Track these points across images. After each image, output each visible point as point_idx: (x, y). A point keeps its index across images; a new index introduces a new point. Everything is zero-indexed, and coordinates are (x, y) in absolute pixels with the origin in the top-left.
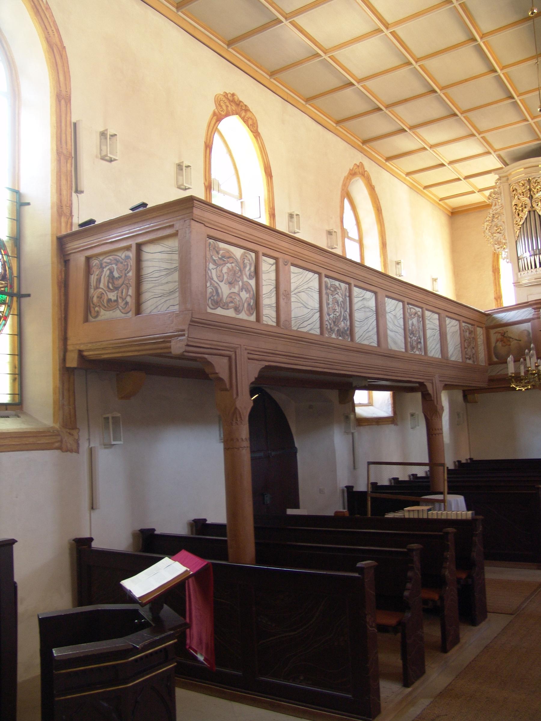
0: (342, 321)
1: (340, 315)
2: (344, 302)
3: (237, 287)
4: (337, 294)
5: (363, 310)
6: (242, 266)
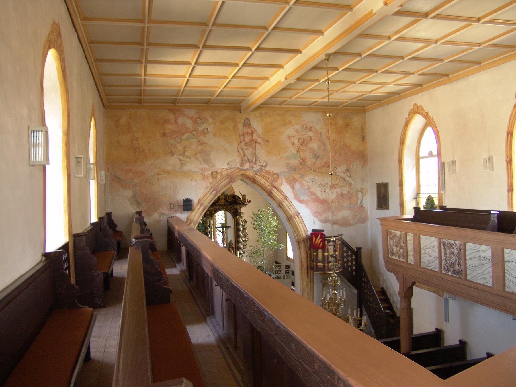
0: (457, 265)
1: (455, 262)
2: (459, 253)
3: (399, 247)
5: (478, 259)
6: (400, 239)
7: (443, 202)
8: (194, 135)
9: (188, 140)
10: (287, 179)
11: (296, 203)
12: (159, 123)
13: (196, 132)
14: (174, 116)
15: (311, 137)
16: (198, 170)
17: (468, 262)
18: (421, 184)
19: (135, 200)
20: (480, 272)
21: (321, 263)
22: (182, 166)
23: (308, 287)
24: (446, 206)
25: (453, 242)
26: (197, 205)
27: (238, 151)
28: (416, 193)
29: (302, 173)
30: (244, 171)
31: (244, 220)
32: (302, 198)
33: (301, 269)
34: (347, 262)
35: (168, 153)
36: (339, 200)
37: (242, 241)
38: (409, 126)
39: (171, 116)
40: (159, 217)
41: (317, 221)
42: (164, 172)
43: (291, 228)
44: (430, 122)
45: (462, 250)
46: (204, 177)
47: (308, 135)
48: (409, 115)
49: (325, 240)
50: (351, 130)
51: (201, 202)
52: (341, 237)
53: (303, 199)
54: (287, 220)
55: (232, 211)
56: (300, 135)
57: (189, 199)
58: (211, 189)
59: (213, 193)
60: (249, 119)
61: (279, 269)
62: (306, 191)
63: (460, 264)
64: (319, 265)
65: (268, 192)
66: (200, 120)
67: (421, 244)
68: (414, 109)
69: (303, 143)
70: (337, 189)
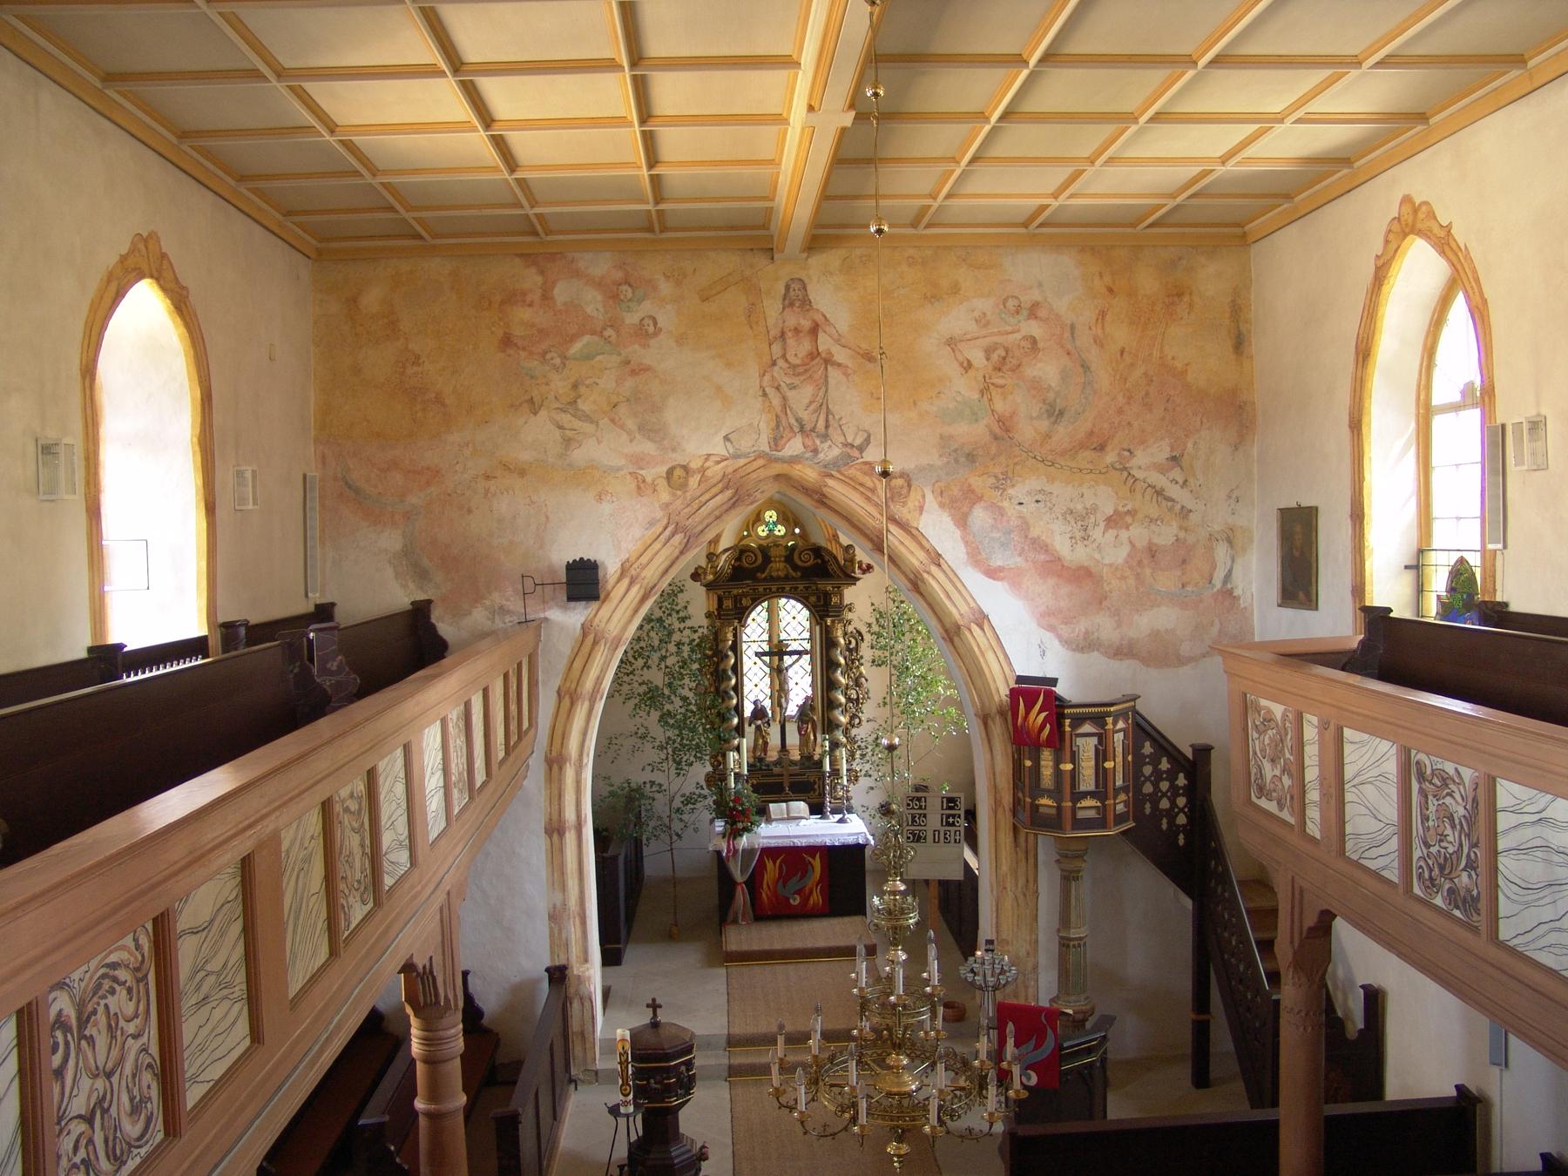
0: (1464, 870)
2: (1471, 819)
4: (1448, 794)
5: (1539, 854)
7: (1498, 587)
8: (607, 340)
9: (589, 357)
10: (942, 493)
11: (973, 580)
12: (490, 305)
13: (618, 332)
14: (539, 279)
15: (1034, 341)
16: (623, 462)
17: (1504, 863)
18: (1437, 510)
19: (412, 563)
20: (1547, 913)
21: (1050, 797)
22: (567, 448)
23: (1016, 880)
24: (1506, 605)
25: (1449, 768)
26: (618, 581)
27: (765, 395)
28: (1414, 548)
29: (998, 470)
30: (785, 465)
32: (997, 561)
33: (993, 815)
34: (1155, 798)
35: (521, 405)
36: (1139, 571)
37: (843, 700)
38: (1385, 289)
39: (531, 279)
40: (489, 619)
41: (1053, 645)
42: (506, 467)
43: (960, 667)
44: (1455, 263)
45: (1484, 808)
46: (642, 487)
47: (1023, 333)
48: (1387, 242)
49: (1061, 716)
50: (1189, 313)
51: (633, 572)
52: (1132, 703)
53: (999, 563)
54: (943, 638)
56: (992, 334)
57: (589, 560)
58: (665, 529)
59: (672, 541)
60: (800, 280)
61: (920, 808)
62: (1015, 536)
63: (1475, 869)
64: (1042, 805)
65: (875, 539)
66: (630, 290)
67: (1346, 761)
68: (1402, 219)
69: (1005, 362)
70: (1131, 528)
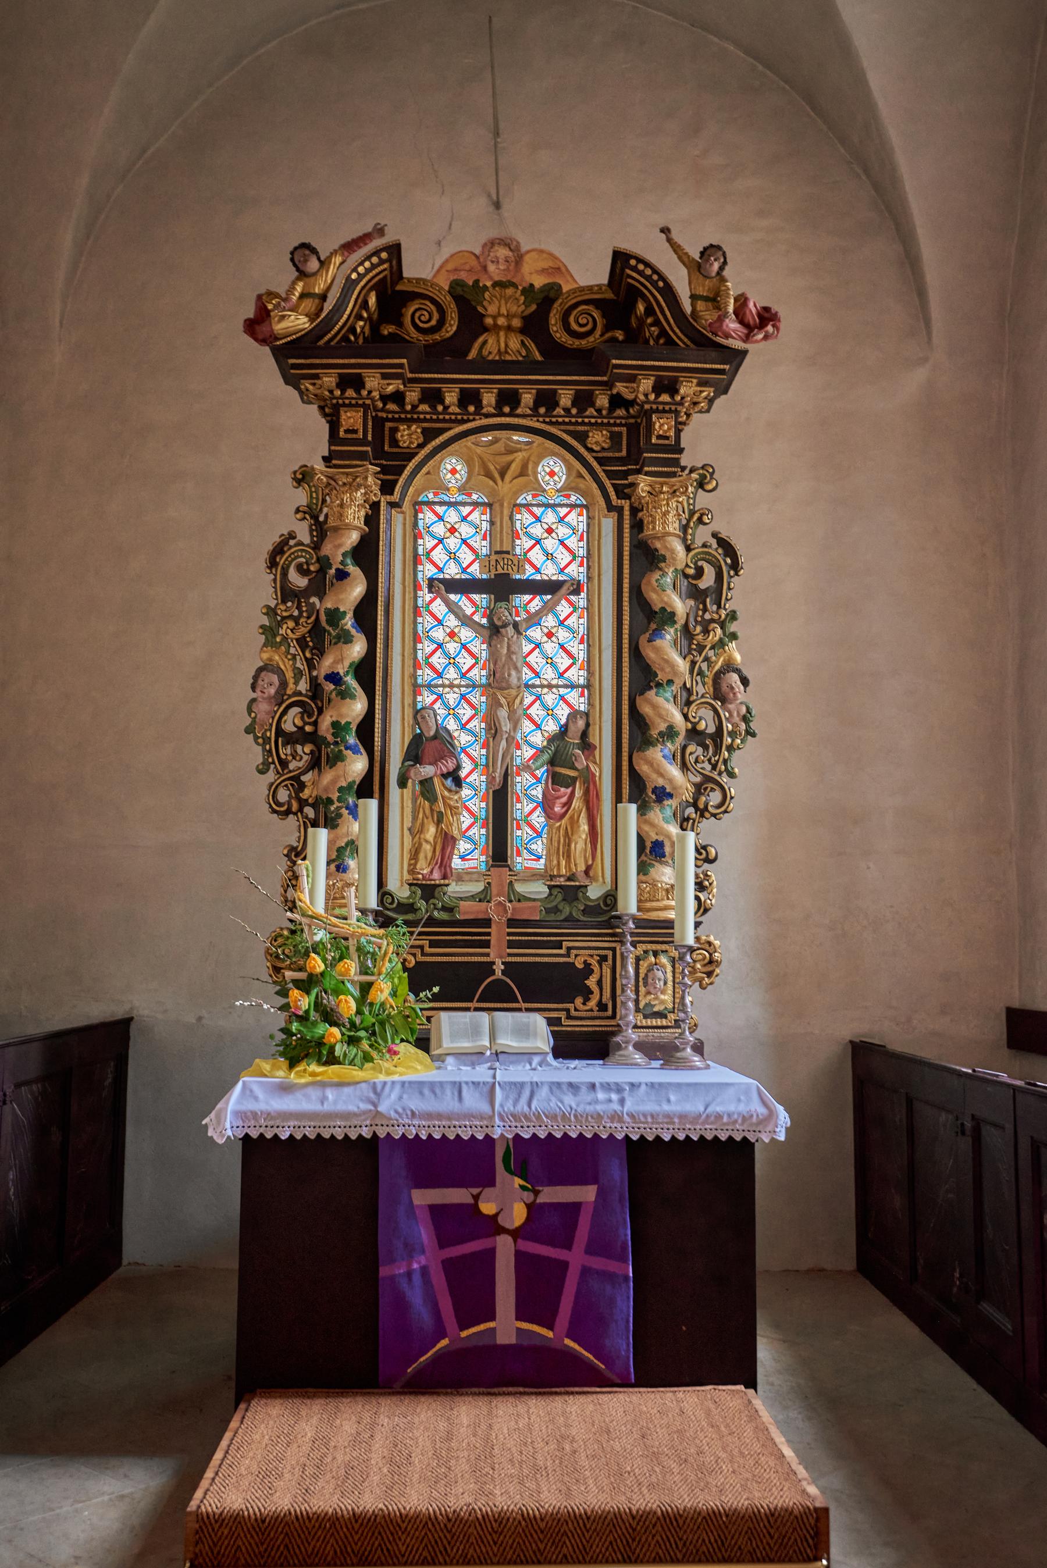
31: (715, 535)
55: (598, 438)
